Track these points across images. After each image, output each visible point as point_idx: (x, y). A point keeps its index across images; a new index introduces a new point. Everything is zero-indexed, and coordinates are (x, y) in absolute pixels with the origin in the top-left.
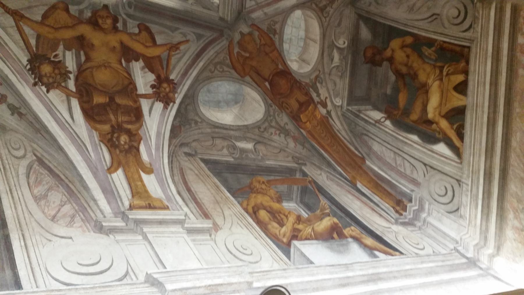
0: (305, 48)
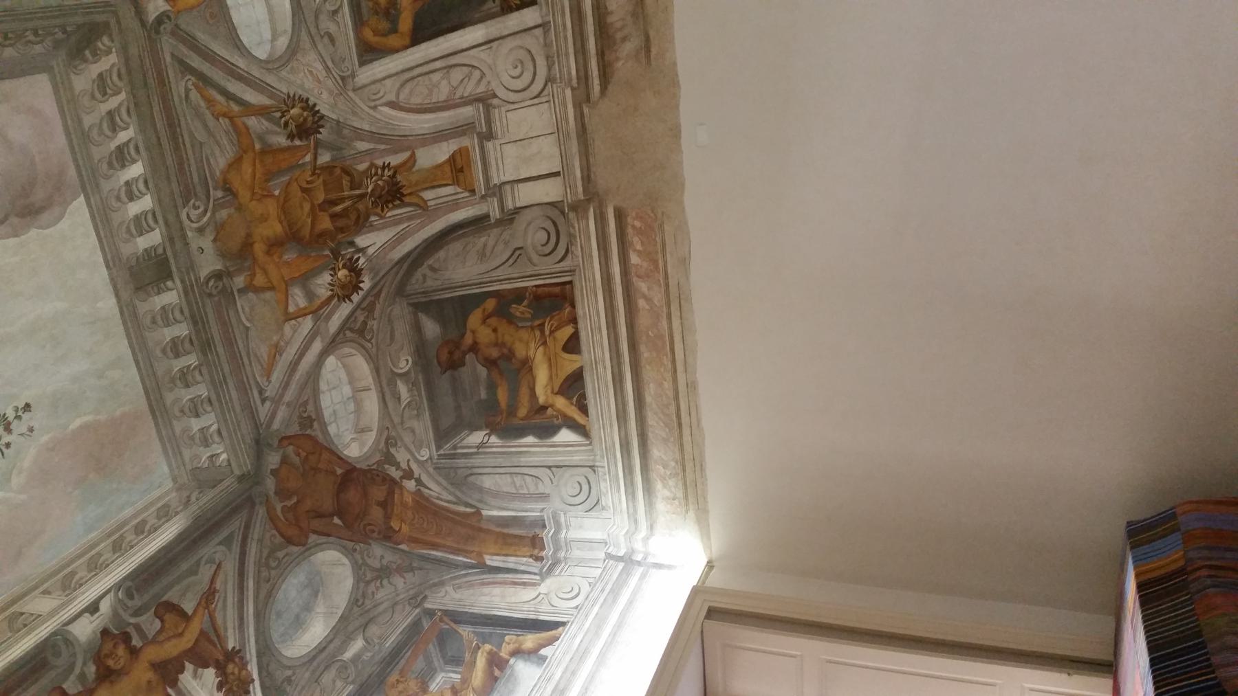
0: (359, 410)
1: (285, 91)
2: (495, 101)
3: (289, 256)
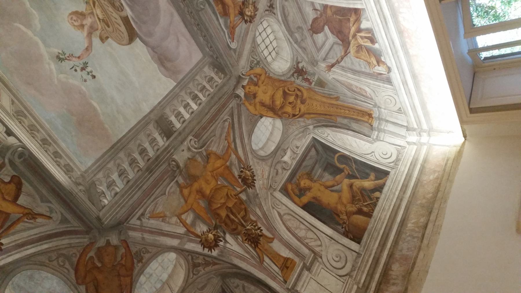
1: (251, 164)
2: (320, 259)
3: (202, 203)
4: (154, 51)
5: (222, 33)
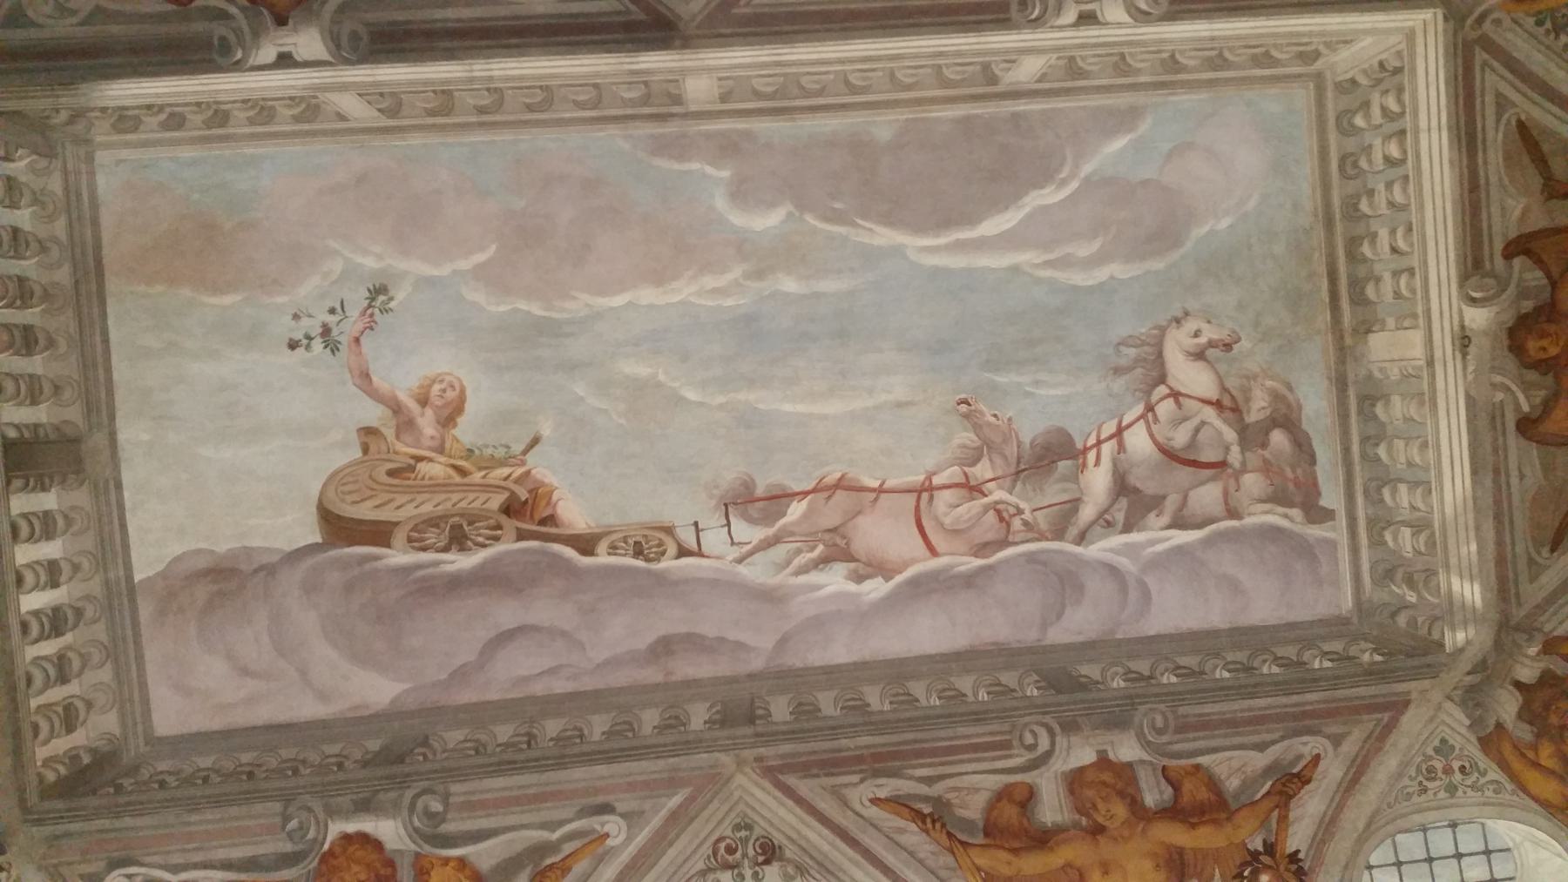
4: (261, 568)
5: (177, 859)
